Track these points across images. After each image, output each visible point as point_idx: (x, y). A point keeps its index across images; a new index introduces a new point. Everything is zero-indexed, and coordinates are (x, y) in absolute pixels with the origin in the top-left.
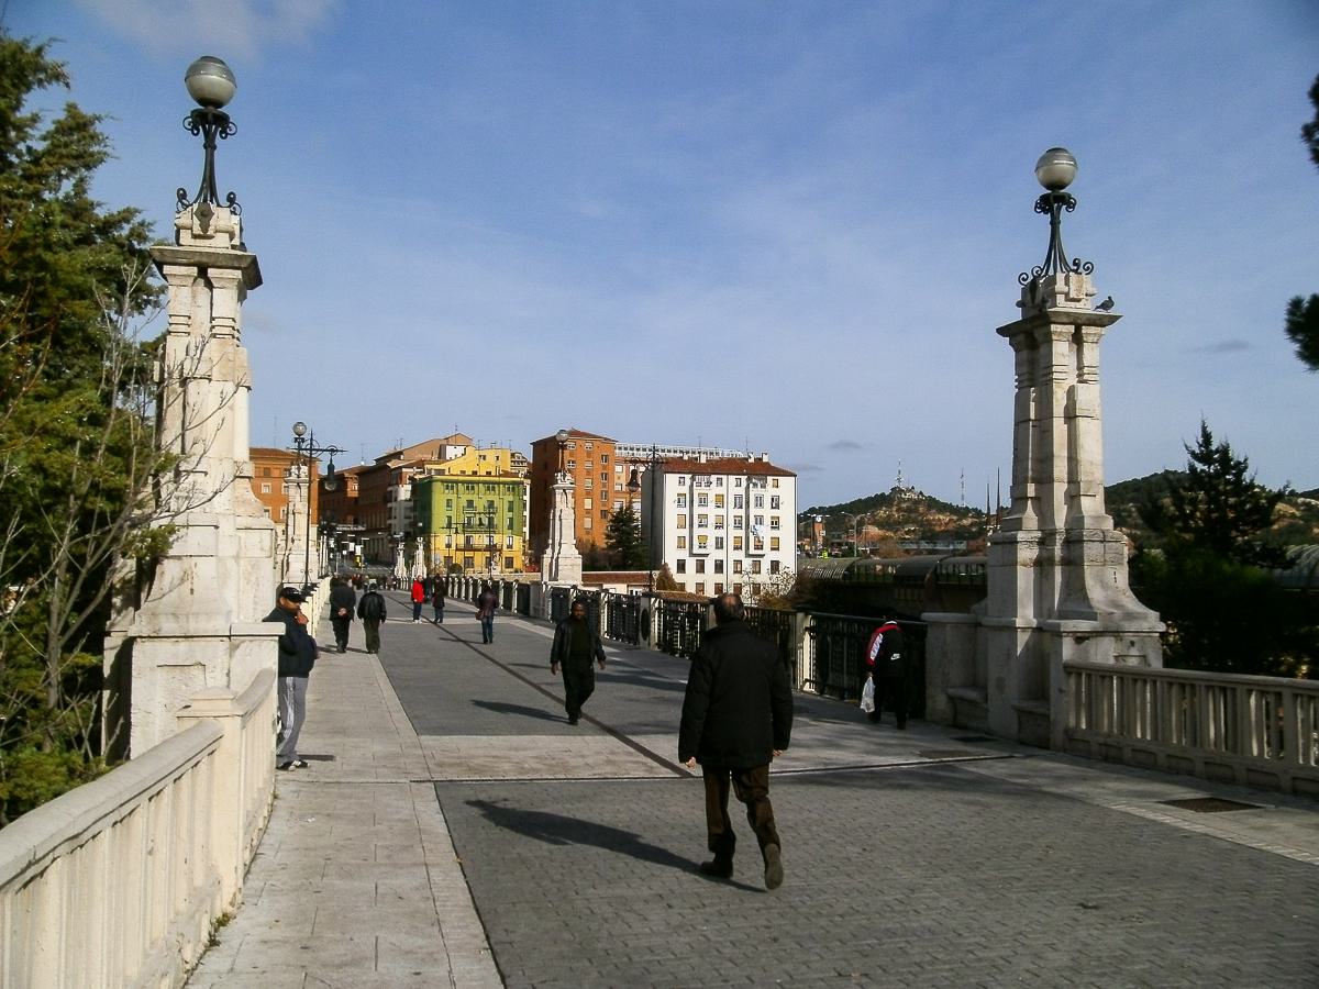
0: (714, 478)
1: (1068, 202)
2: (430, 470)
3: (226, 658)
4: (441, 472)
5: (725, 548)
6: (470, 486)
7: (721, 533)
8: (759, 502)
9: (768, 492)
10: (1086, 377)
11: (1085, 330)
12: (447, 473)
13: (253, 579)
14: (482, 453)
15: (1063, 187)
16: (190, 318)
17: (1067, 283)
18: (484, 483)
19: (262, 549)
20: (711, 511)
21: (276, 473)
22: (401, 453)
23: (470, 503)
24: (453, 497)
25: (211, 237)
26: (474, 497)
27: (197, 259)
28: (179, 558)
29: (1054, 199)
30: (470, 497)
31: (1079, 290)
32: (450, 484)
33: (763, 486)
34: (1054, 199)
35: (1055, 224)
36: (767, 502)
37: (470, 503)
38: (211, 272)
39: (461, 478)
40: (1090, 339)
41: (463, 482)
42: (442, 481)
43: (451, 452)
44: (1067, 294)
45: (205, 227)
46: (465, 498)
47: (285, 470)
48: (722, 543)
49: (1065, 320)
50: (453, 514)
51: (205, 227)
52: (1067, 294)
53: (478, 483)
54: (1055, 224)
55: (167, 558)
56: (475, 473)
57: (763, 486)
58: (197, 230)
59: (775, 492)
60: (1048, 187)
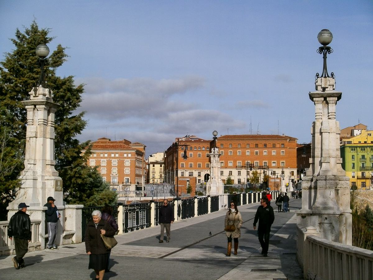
1: (328, 49)
2: (345, 142)
4: (350, 142)
6: (363, 148)
12: (353, 143)
14: (369, 132)
15: (328, 44)
16: (33, 120)
18: (370, 147)
19: (51, 186)
21: (278, 146)
23: (363, 157)
24: (355, 154)
25: (38, 96)
26: (365, 154)
27: (32, 103)
28: (24, 188)
29: (325, 49)
30: (363, 154)
31: (326, 84)
32: (354, 148)
34: (325, 49)
35: (325, 58)
37: (363, 157)
39: (359, 145)
40: (331, 102)
41: (359, 147)
42: (350, 147)
43: (356, 132)
45: (36, 94)
46: (361, 154)
47: (282, 144)
49: (318, 96)
50: (355, 162)
51: (36, 95)
53: (367, 147)
54: (325, 58)
56: (365, 142)
60: (322, 44)
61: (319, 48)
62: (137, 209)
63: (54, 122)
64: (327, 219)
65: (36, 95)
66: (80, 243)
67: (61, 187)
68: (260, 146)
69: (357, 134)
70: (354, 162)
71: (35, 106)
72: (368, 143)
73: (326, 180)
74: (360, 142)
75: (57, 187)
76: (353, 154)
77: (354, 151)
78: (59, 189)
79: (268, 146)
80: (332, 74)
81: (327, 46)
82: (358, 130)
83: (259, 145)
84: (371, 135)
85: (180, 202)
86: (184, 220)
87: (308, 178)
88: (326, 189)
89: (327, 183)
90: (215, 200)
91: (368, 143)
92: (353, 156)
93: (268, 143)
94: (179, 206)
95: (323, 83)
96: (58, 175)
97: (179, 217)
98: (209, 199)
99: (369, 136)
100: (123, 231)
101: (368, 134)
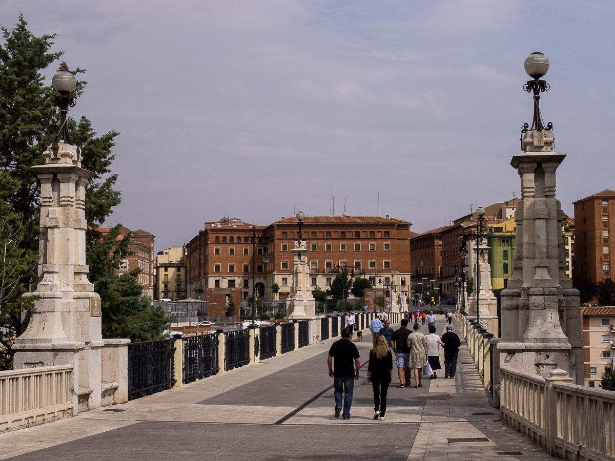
1: (543, 85)
2: (491, 229)
3: (52, 359)
4: (499, 230)
10: (547, 193)
11: (544, 165)
12: (504, 230)
13: (81, 322)
15: (541, 75)
17: (532, 137)
21: (378, 235)
22: (471, 215)
24: (508, 248)
27: (51, 171)
28: (40, 313)
29: (537, 85)
31: (540, 140)
34: (537, 85)
35: (537, 99)
38: (59, 176)
40: (549, 170)
42: (499, 237)
44: (532, 143)
45: (55, 154)
49: (527, 160)
50: (509, 262)
51: (55, 154)
52: (532, 143)
54: (537, 99)
55: (35, 313)
58: (52, 156)
60: (532, 76)
61: (528, 82)
62: (200, 344)
63: (84, 202)
64: (550, 357)
65: (57, 156)
66: (126, 402)
67: (98, 310)
68: (348, 235)
69: (511, 216)
70: (506, 261)
71: (55, 175)
73: (543, 295)
75: (94, 310)
77: (506, 244)
78: (96, 313)
79: (362, 236)
80: (550, 124)
81: (540, 79)
82: (513, 209)
83: (347, 234)
85: (257, 331)
86: (263, 361)
87: (513, 291)
88: (544, 309)
89: (546, 300)
90: (304, 325)
92: (505, 252)
93: (363, 230)
94: (257, 337)
95: (536, 139)
96: (93, 290)
97: (257, 356)
98: (296, 326)
100: (183, 381)
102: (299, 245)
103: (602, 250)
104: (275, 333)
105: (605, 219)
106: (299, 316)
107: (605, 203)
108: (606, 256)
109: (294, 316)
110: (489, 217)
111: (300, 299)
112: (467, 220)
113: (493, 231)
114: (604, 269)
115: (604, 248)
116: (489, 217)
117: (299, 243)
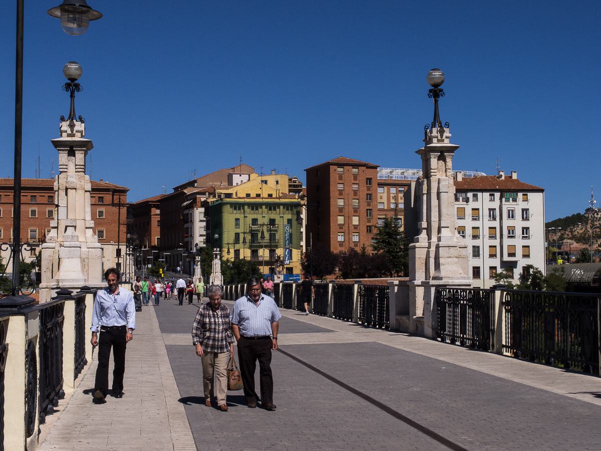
0: (470, 195)
4: (229, 196)
5: (481, 256)
6: (255, 206)
7: (477, 242)
8: (511, 215)
9: (519, 205)
12: (234, 196)
14: (264, 178)
20: (468, 223)
22: (195, 181)
23: (255, 221)
24: (241, 217)
26: (259, 217)
30: (255, 216)
32: (237, 206)
33: (515, 200)
36: (518, 214)
37: (255, 221)
46: (251, 217)
48: (479, 251)
56: (258, 196)
57: (515, 200)
59: (525, 205)
69: (237, 184)
72: (263, 198)
74: (248, 195)
76: (238, 216)
77: (239, 211)
82: (240, 176)
84: (268, 182)
91: (263, 198)
92: (237, 220)
99: (264, 184)
101: (262, 181)
102: (72, 131)
103: (337, 220)
104: (61, 325)
105: (340, 187)
106: (73, 280)
107: (341, 169)
108: (341, 226)
109: (63, 280)
110: (217, 183)
111: (73, 244)
112: (190, 186)
113: (223, 196)
114: (339, 240)
115: (339, 217)
116: (217, 183)
117: (72, 126)
